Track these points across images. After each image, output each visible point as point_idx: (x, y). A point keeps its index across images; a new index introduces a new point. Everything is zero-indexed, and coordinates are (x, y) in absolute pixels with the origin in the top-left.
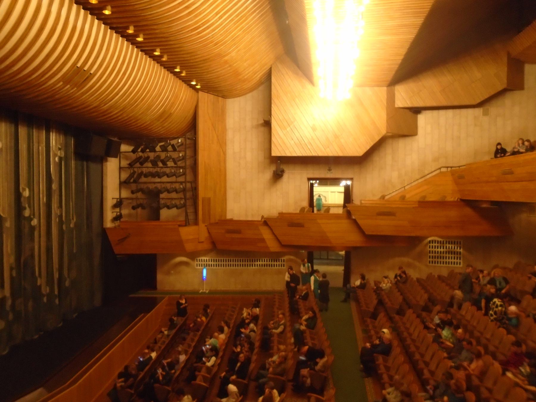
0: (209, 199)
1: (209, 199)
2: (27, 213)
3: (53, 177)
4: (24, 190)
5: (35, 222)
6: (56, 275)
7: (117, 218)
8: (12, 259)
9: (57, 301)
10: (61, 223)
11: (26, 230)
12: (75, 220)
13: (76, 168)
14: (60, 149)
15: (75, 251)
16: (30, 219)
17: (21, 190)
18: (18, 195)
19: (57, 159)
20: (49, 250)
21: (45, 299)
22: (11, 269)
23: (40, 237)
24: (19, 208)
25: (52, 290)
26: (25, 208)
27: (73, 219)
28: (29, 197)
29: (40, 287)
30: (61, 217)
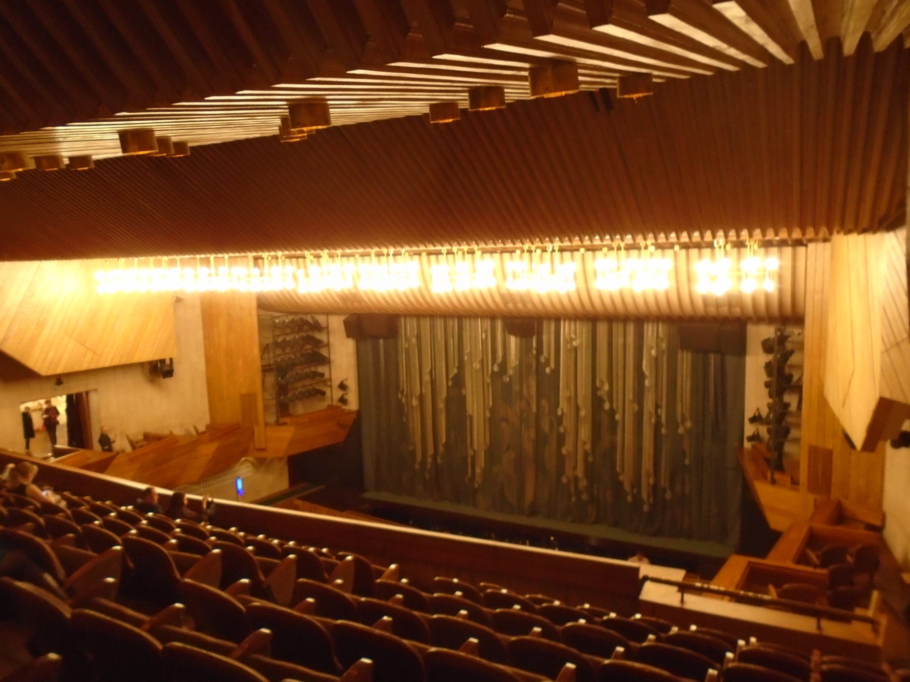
0: (829, 454)
1: (829, 454)
2: (607, 406)
3: (647, 373)
4: (602, 383)
5: (618, 417)
6: (647, 481)
7: (755, 438)
8: (588, 447)
9: (646, 508)
10: (657, 426)
11: (605, 421)
12: (689, 424)
13: (694, 364)
14: (663, 340)
15: (687, 462)
16: (612, 412)
17: (598, 384)
18: (595, 389)
19: (653, 352)
20: (639, 450)
21: (629, 498)
22: (586, 454)
23: (624, 432)
24: (596, 402)
25: (639, 491)
26: (604, 401)
27: (683, 423)
28: (610, 393)
29: (621, 484)
30: (658, 417)
